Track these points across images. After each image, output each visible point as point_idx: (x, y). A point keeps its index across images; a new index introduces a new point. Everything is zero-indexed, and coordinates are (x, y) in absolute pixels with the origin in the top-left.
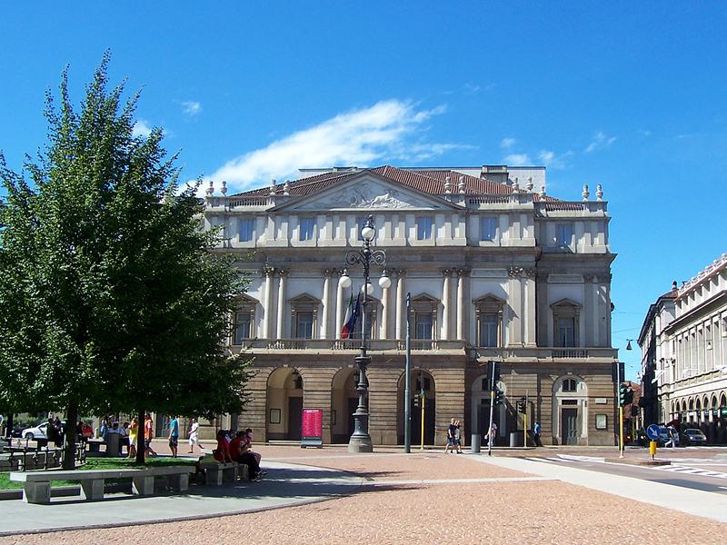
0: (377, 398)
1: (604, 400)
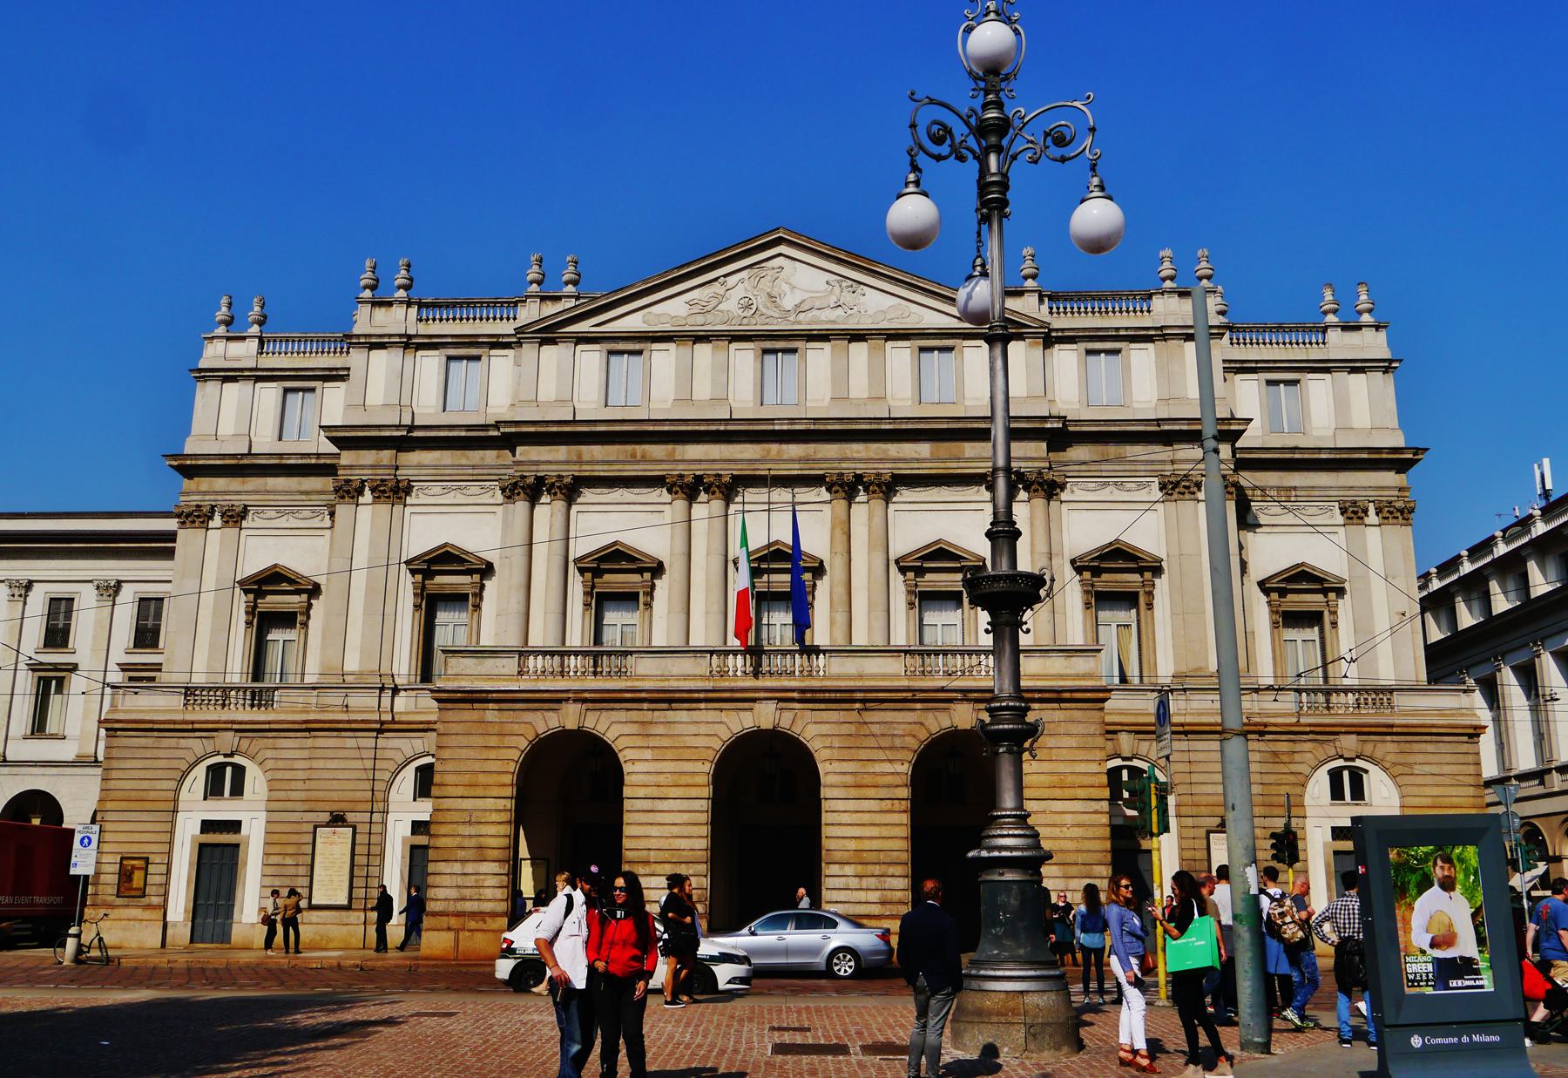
0: (845, 818)
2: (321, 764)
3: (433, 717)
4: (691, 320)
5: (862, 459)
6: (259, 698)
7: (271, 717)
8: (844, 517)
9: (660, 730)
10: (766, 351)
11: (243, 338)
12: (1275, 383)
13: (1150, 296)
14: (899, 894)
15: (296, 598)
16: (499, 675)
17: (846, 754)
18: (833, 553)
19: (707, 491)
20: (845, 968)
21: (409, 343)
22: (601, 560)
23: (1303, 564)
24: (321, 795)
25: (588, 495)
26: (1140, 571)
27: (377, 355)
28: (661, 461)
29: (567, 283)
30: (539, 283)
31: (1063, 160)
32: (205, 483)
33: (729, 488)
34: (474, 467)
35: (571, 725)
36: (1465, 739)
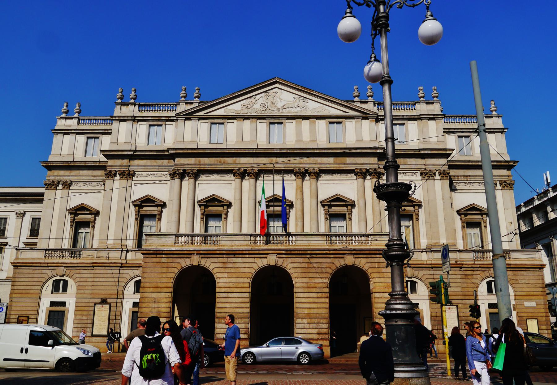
0: (304, 300)
1: (533, 304)
2: (97, 280)
3: (141, 262)
4: (242, 112)
5: (306, 163)
6: (74, 253)
7: (79, 261)
8: (301, 185)
9: (230, 265)
10: (271, 123)
11: (72, 118)
12: (461, 137)
13: (415, 104)
14: (325, 330)
15: (90, 216)
16: (167, 244)
17: (304, 275)
18: (296, 199)
19: (248, 175)
20: (305, 360)
21: (135, 119)
22: (207, 201)
23: (473, 204)
24: (98, 292)
25: (203, 177)
26: (414, 206)
27: (123, 124)
28: (231, 164)
29: (195, 97)
30: (185, 97)
31: (414, 6)
32: (56, 173)
33: (257, 174)
34: (159, 166)
35: (195, 263)
36: (538, 269)
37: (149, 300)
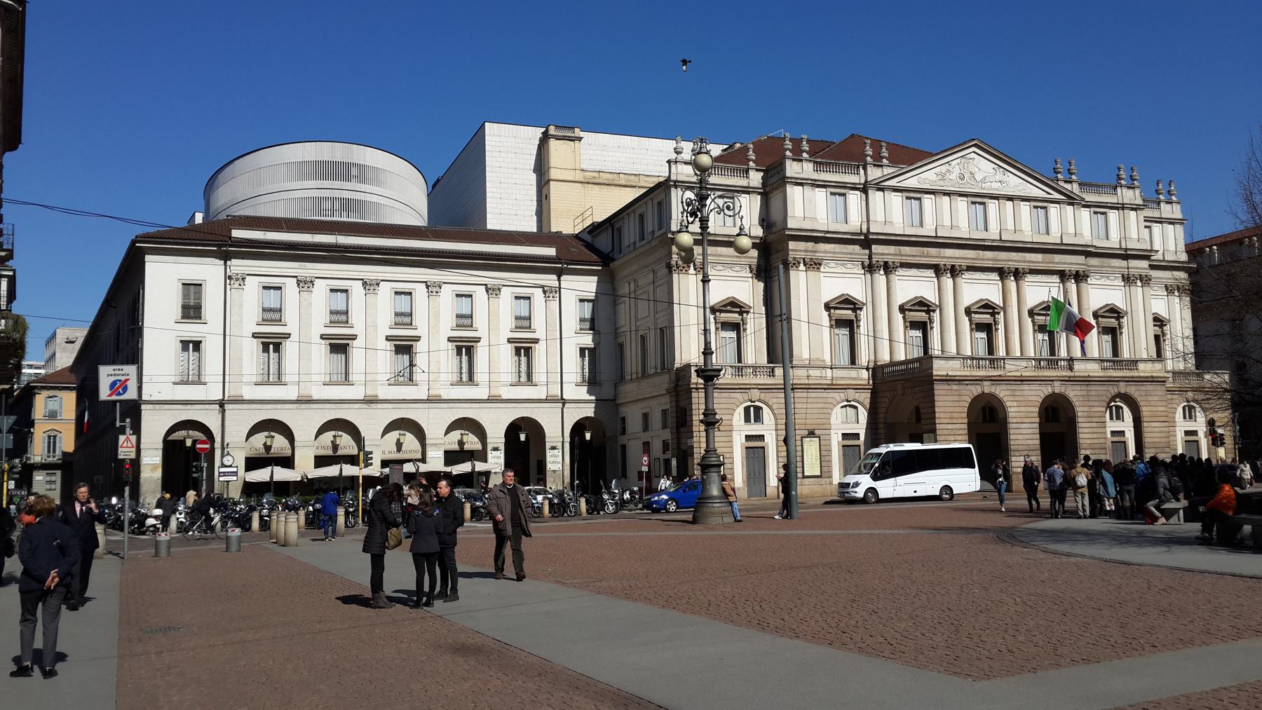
9: (1018, 393)
21: (816, 184)
37: (946, 432)
